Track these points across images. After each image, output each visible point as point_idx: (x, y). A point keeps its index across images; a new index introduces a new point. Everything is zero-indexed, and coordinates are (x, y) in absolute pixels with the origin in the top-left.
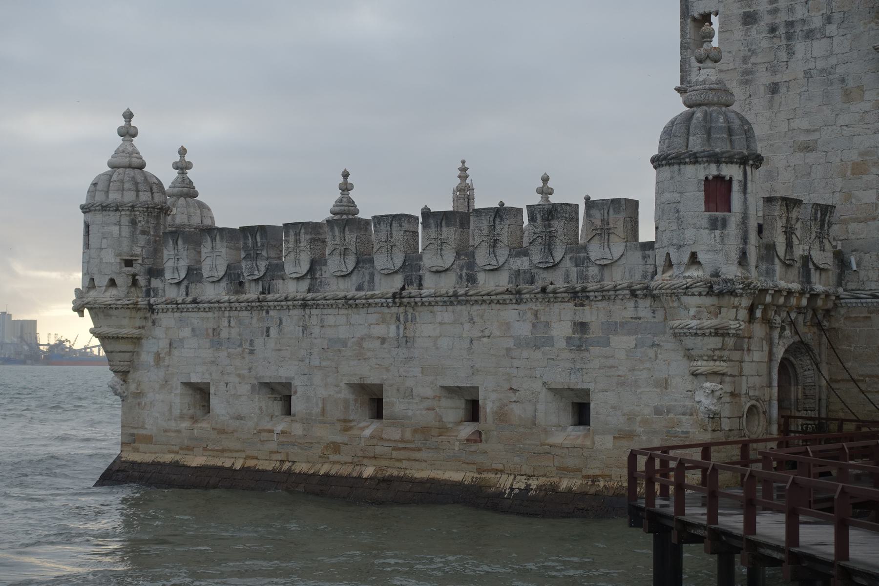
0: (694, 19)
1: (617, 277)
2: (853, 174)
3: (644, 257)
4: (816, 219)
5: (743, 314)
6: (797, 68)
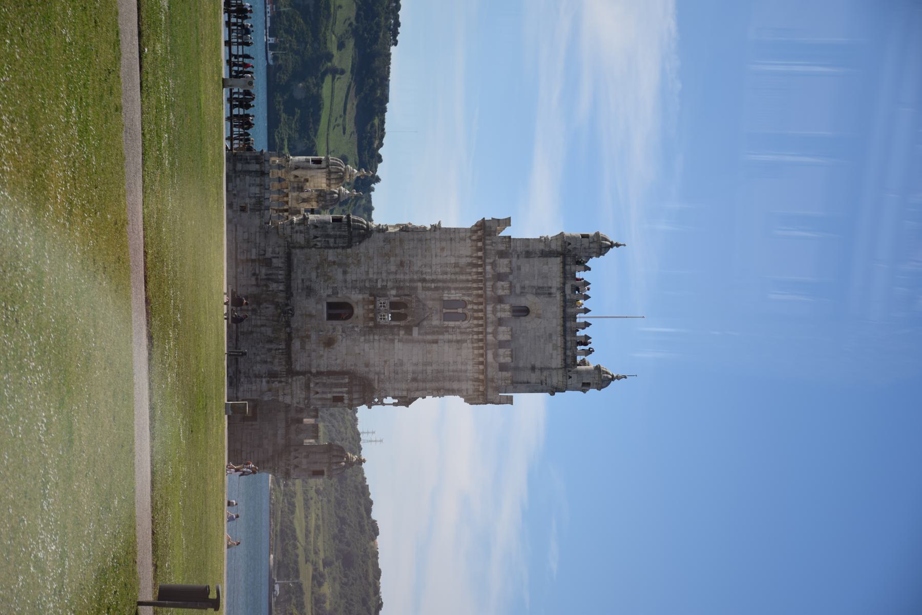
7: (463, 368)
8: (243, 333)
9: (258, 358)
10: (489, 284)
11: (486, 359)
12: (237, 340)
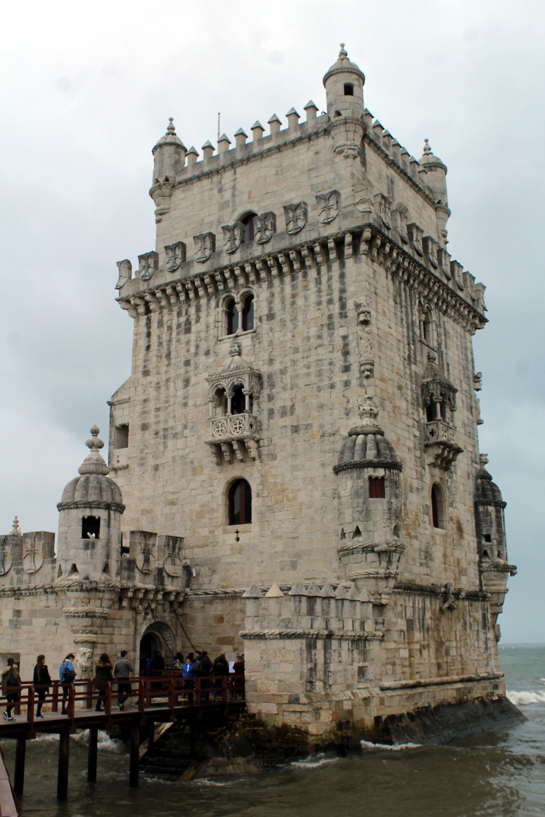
0: (117, 428)
1: (38, 581)
2: (197, 518)
3: (53, 568)
4: (169, 545)
5: (106, 603)
6: (168, 455)
7: (459, 338)
9: (476, 645)
10: (417, 257)
11: (465, 302)
12: (470, 680)
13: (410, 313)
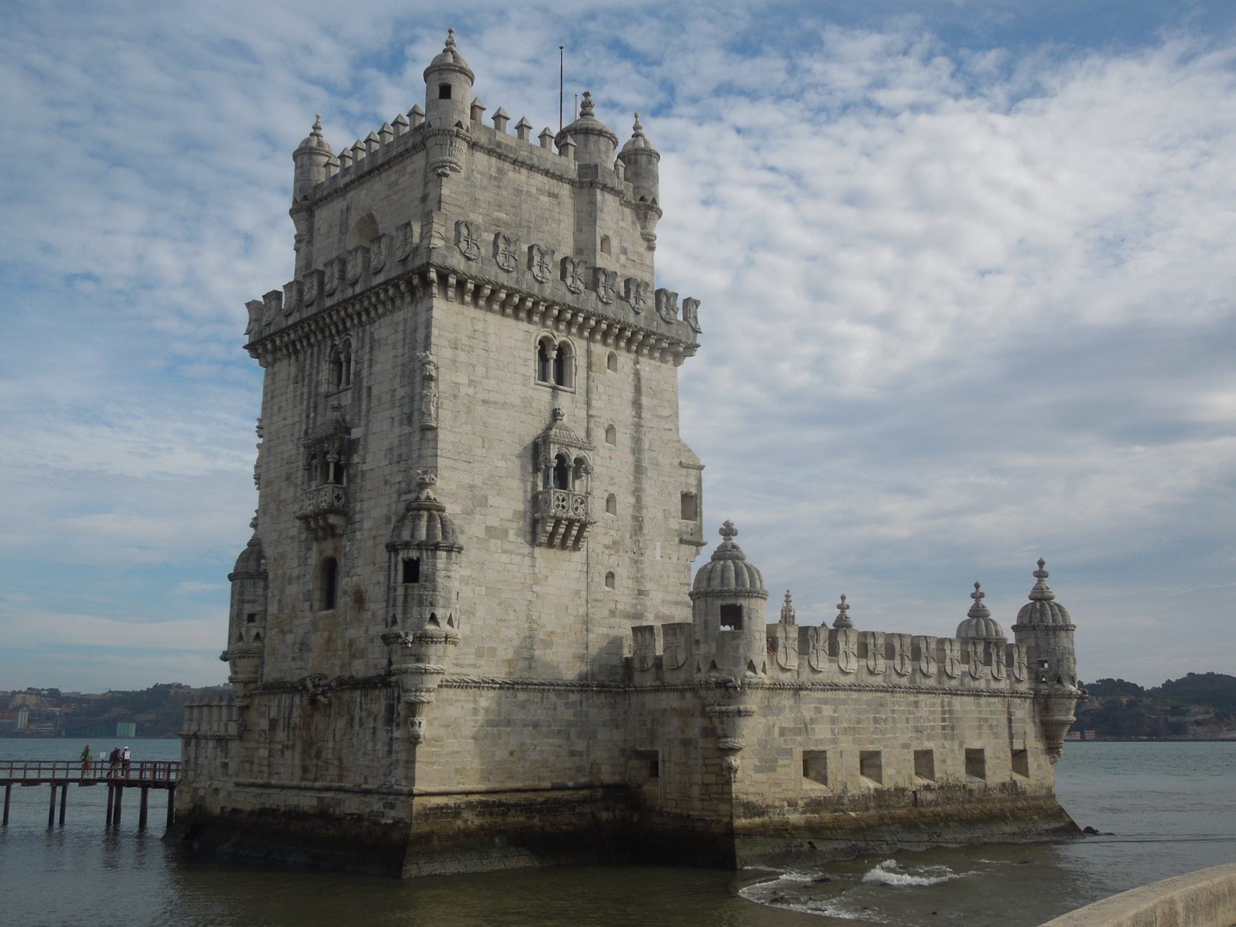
7: (401, 328)
8: (341, 777)
9: (370, 746)
11: (378, 286)
13: (314, 377)
